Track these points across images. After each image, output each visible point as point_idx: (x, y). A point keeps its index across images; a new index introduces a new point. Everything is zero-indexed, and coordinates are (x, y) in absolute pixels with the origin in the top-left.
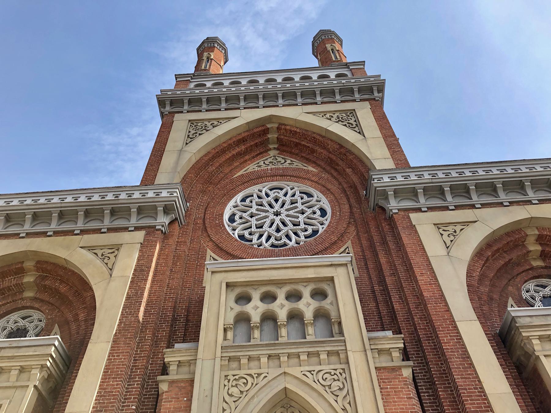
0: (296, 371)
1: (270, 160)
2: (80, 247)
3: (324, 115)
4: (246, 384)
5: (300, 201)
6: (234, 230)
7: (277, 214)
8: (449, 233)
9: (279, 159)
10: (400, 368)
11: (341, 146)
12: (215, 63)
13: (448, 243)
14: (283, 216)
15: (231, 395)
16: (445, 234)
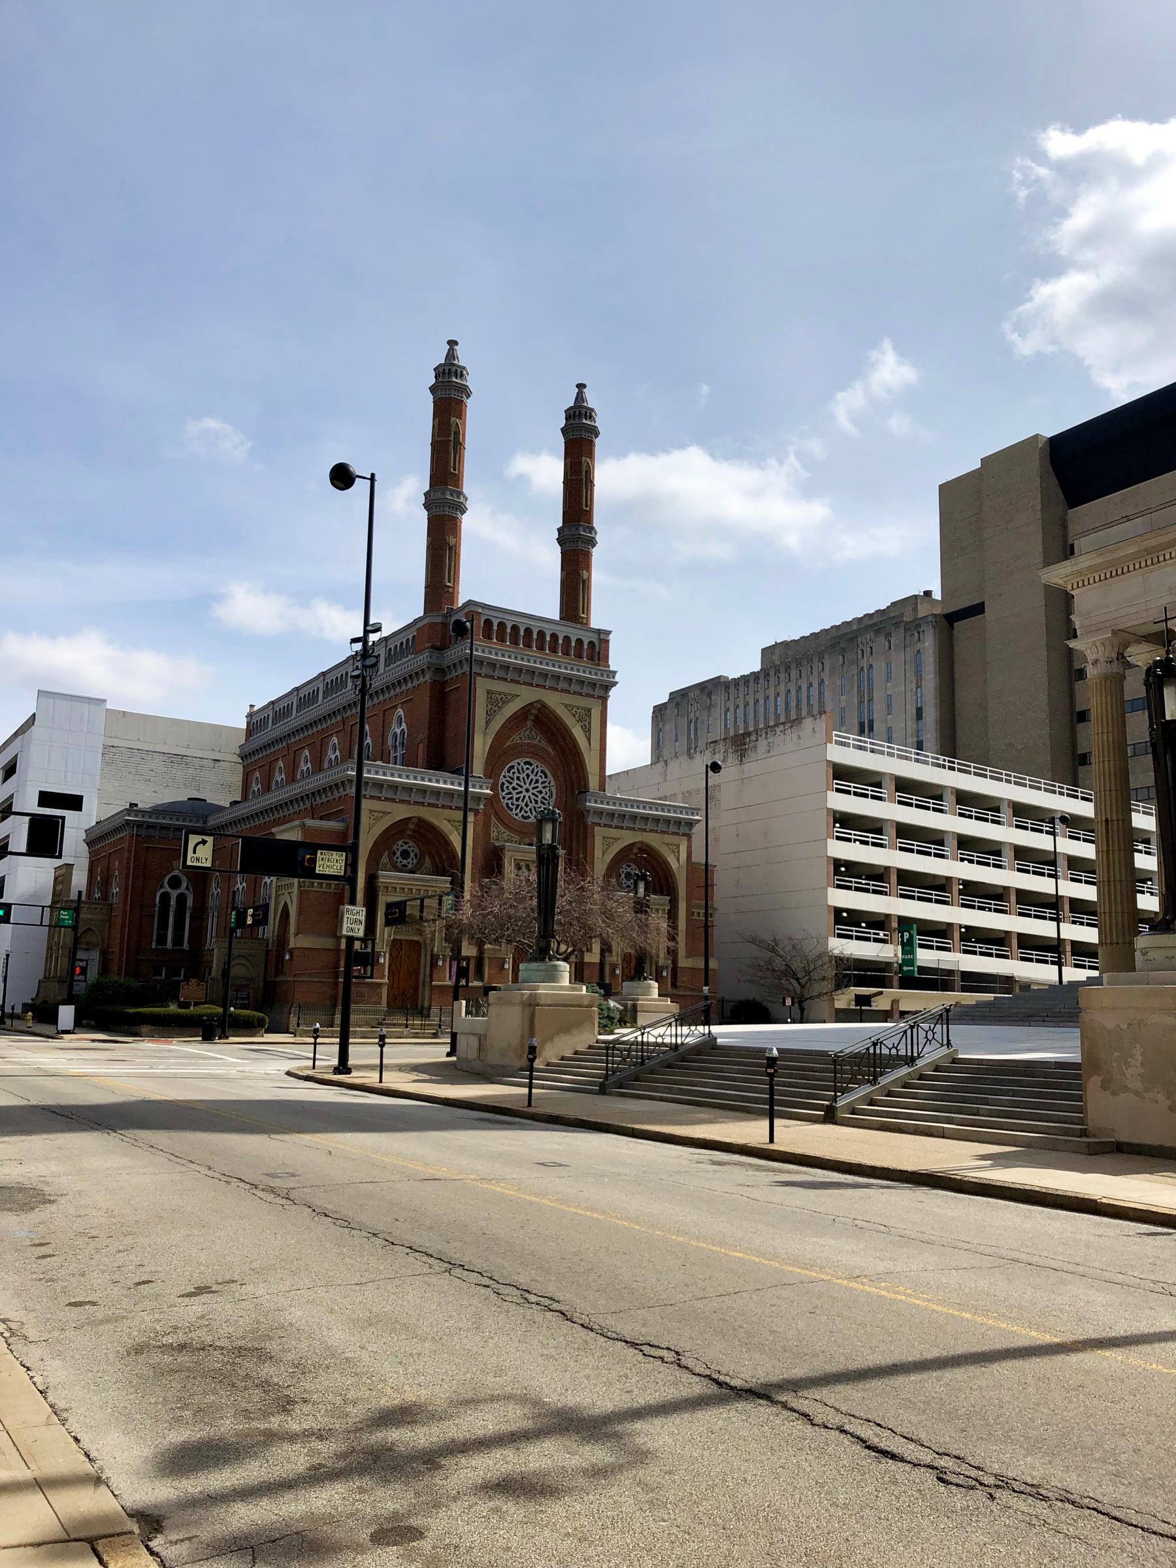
1: (528, 732)
5: (540, 781)
7: (527, 790)
9: (533, 733)
11: (575, 747)
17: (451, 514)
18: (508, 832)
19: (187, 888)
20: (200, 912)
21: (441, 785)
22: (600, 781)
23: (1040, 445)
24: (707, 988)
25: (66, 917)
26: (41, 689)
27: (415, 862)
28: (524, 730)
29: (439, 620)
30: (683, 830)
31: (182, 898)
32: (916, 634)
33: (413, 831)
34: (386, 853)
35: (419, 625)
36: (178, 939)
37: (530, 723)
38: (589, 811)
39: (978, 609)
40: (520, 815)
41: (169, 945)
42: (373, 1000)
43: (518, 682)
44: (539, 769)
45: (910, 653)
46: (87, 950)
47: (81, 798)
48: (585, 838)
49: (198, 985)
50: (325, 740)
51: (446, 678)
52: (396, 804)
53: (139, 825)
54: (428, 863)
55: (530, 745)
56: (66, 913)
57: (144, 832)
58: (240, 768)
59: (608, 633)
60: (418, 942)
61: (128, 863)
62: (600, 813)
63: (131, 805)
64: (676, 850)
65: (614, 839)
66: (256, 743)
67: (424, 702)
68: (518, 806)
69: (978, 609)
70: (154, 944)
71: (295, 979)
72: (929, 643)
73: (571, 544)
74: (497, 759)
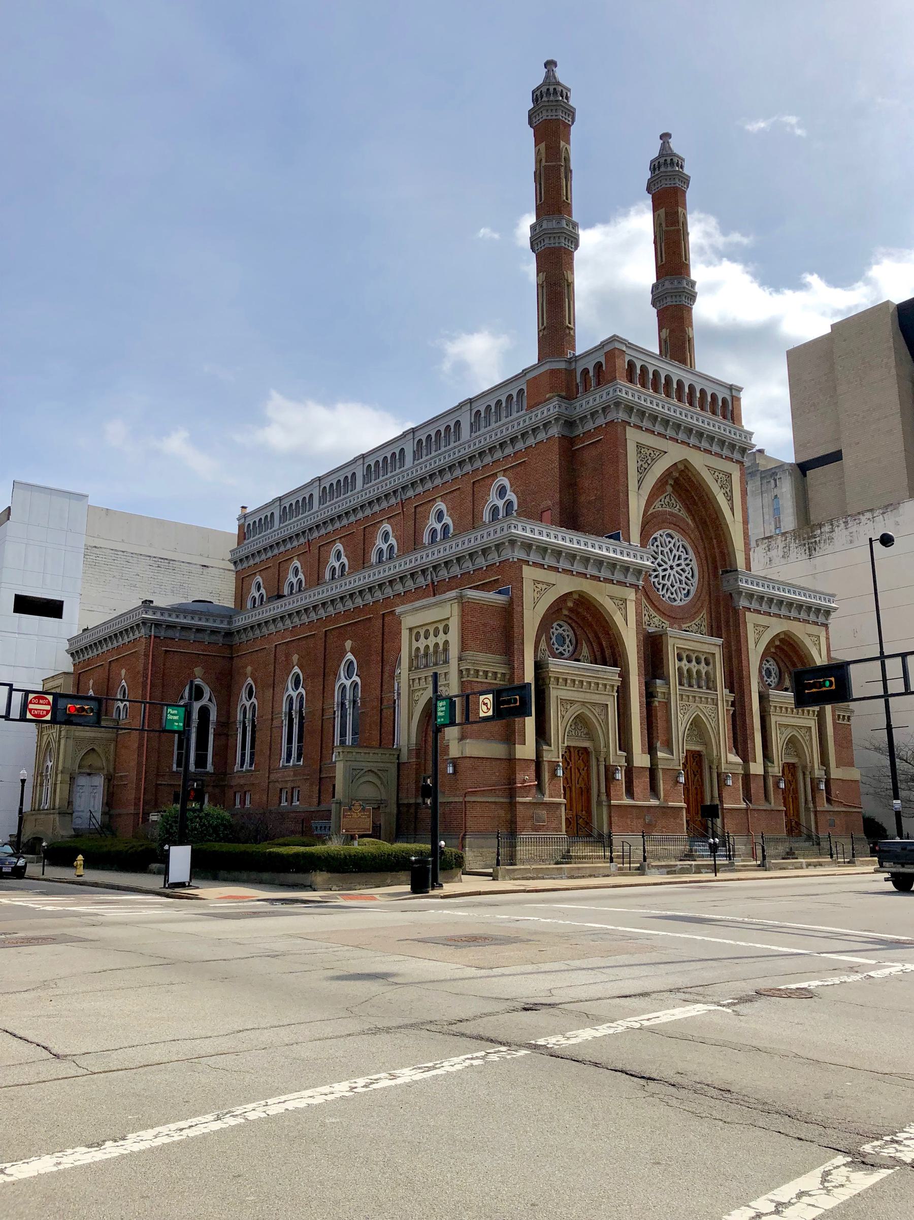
0: (701, 706)
1: (667, 499)
7: (671, 567)
9: (673, 501)
12: (656, 354)
16: (756, 632)
17: (566, 247)
18: (658, 617)
19: (210, 700)
20: (226, 726)
21: (605, 553)
23: (891, 311)
24: (899, 802)
25: (176, 718)
26: (18, 479)
27: (571, 648)
28: (664, 495)
29: (562, 366)
30: (821, 619)
31: (204, 711)
32: (772, 482)
33: (571, 610)
35: (529, 376)
36: (201, 761)
37: (669, 489)
38: (740, 593)
39: (836, 456)
40: (667, 596)
41: (192, 768)
42: (553, 825)
43: (665, 437)
44: (680, 543)
45: (767, 498)
46: (89, 774)
47: (61, 603)
48: (737, 625)
49: (364, 809)
50: (419, 509)
51: (577, 433)
53: (157, 624)
54: (585, 651)
56: (176, 712)
57: (162, 634)
58: (232, 577)
59: (739, 390)
60: (585, 749)
61: (146, 669)
62: (750, 596)
63: (145, 602)
64: (817, 642)
65: (764, 627)
66: (257, 541)
67: (553, 460)
68: (664, 585)
69: (836, 456)
70: (175, 766)
71: (467, 799)
72: (786, 489)
73: (662, 303)
74: (649, 523)
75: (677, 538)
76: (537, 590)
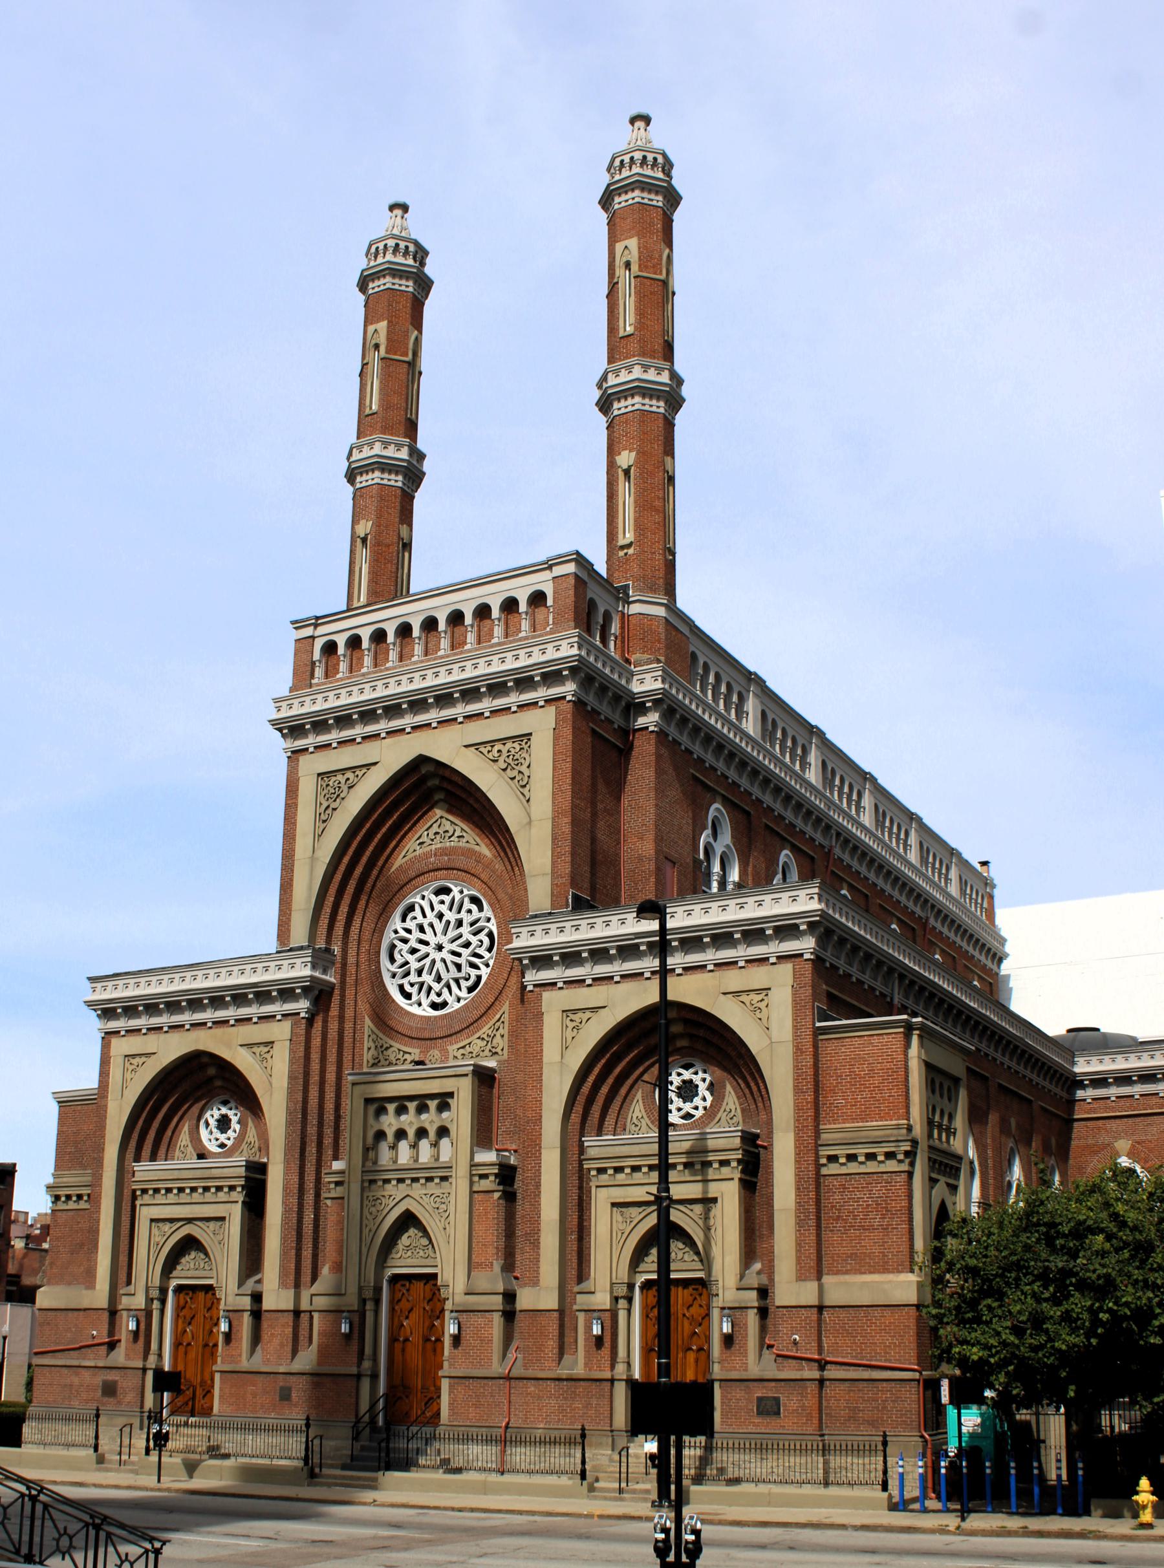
2: (241, 1045)
3: (490, 748)
4: (381, 1204)
6: (394, 976)
8: (574, 1024)
9: (448, 826)
10: (493, 1191)
13: (569, 1039)
14: (448, 947)
15: (371, 1214)
22: (554, 885)
34: (186, 1128)
52: (163, 1036)
55: (444, 852)
75: (418, 899)
76: (131, 1068)
